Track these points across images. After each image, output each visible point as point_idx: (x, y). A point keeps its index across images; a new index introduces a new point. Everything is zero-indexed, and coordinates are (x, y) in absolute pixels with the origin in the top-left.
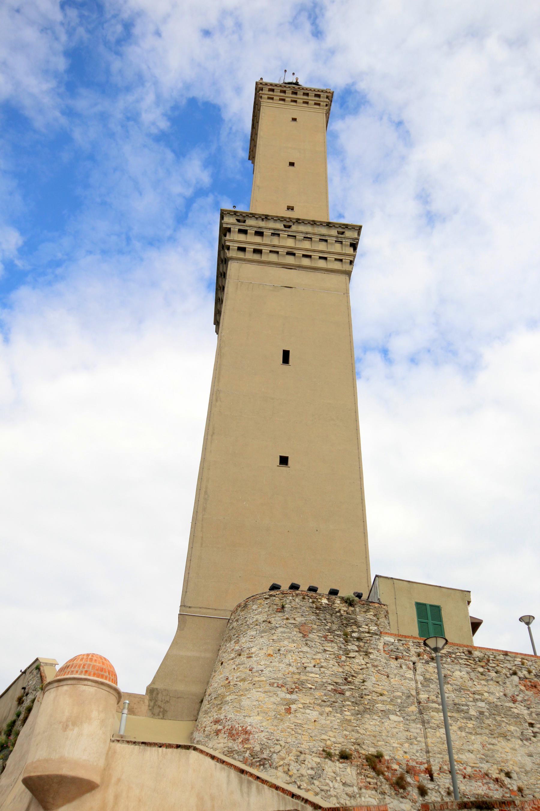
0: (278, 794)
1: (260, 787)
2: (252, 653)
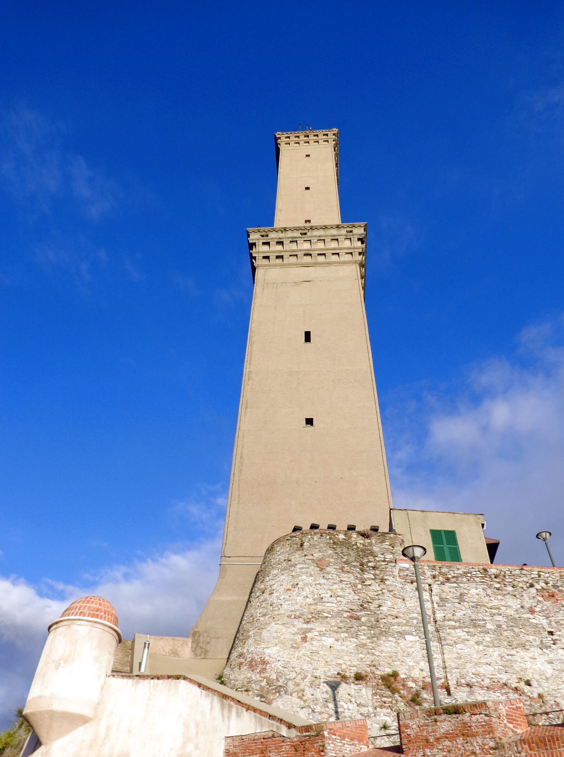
0: (255, 716)
1: (240, 711)
2: (273, 590)
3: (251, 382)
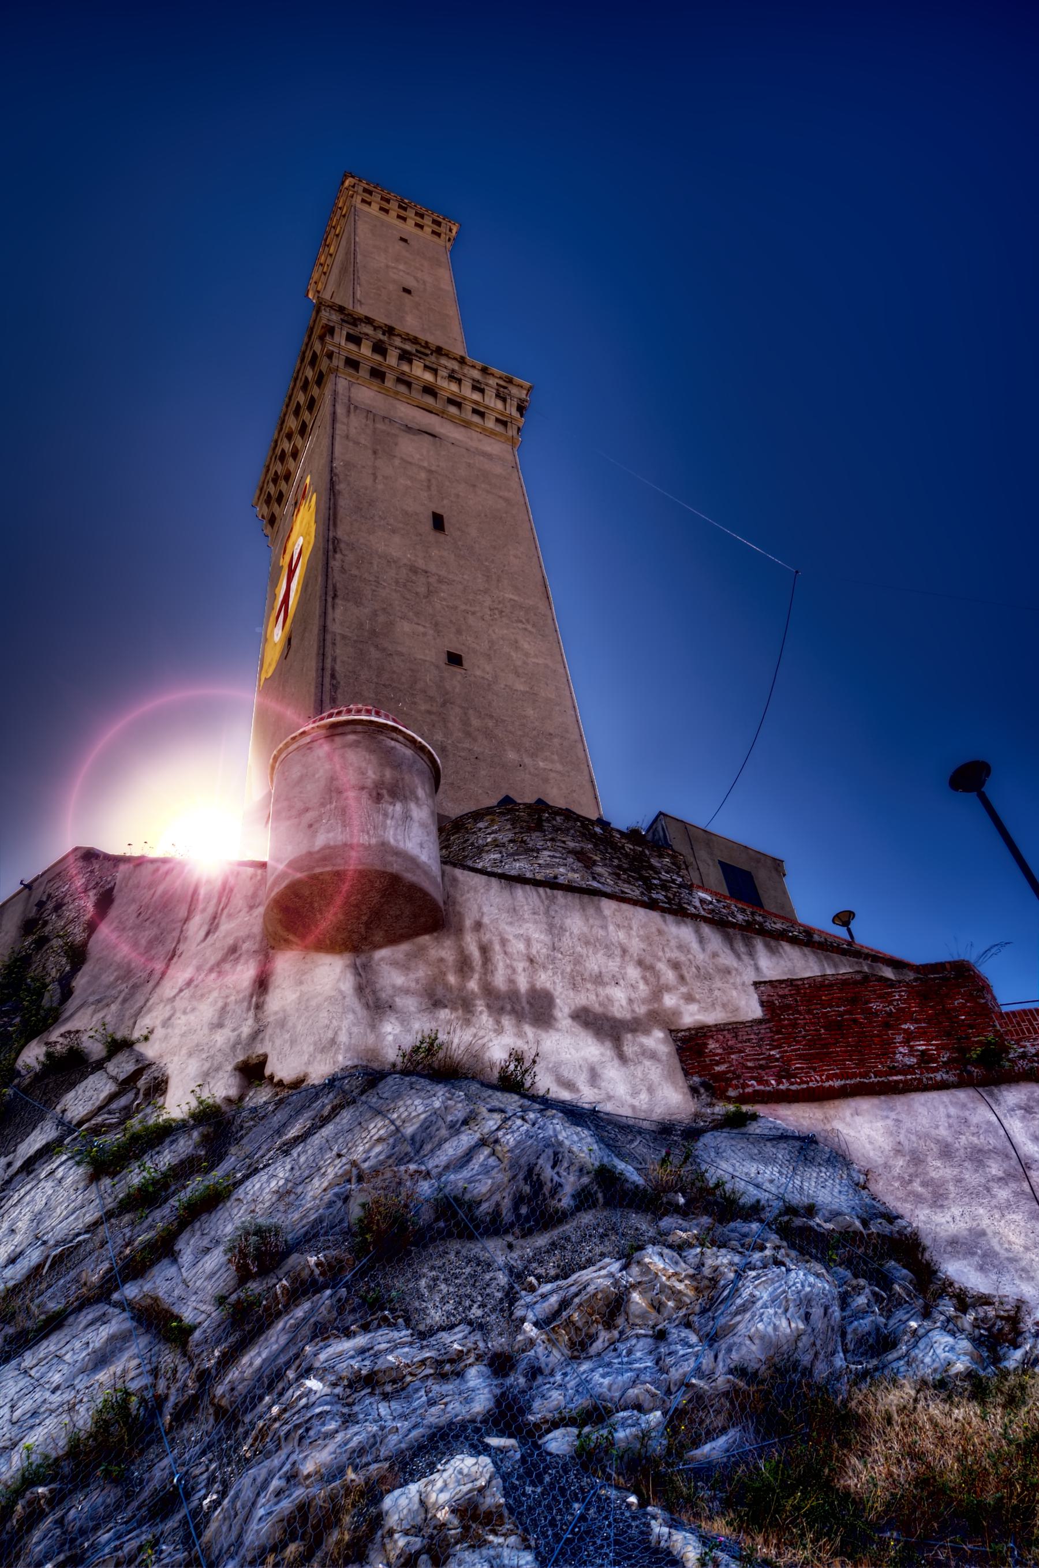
3: (338, 556)
